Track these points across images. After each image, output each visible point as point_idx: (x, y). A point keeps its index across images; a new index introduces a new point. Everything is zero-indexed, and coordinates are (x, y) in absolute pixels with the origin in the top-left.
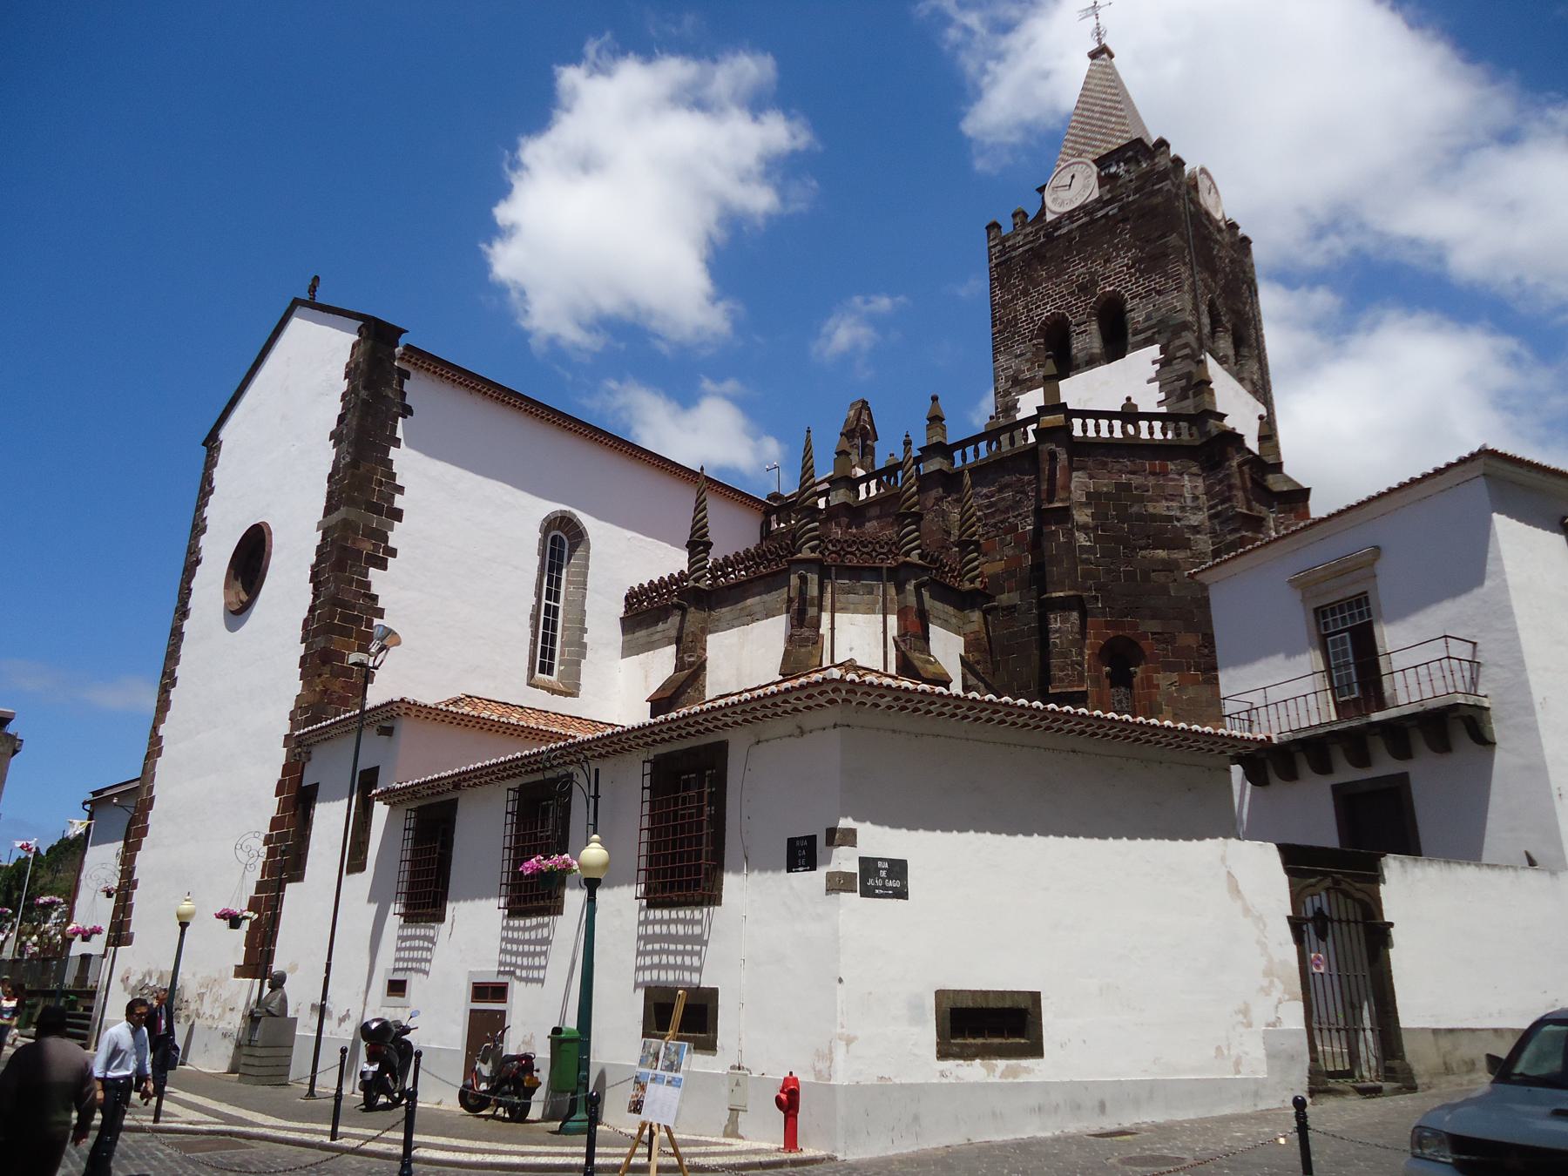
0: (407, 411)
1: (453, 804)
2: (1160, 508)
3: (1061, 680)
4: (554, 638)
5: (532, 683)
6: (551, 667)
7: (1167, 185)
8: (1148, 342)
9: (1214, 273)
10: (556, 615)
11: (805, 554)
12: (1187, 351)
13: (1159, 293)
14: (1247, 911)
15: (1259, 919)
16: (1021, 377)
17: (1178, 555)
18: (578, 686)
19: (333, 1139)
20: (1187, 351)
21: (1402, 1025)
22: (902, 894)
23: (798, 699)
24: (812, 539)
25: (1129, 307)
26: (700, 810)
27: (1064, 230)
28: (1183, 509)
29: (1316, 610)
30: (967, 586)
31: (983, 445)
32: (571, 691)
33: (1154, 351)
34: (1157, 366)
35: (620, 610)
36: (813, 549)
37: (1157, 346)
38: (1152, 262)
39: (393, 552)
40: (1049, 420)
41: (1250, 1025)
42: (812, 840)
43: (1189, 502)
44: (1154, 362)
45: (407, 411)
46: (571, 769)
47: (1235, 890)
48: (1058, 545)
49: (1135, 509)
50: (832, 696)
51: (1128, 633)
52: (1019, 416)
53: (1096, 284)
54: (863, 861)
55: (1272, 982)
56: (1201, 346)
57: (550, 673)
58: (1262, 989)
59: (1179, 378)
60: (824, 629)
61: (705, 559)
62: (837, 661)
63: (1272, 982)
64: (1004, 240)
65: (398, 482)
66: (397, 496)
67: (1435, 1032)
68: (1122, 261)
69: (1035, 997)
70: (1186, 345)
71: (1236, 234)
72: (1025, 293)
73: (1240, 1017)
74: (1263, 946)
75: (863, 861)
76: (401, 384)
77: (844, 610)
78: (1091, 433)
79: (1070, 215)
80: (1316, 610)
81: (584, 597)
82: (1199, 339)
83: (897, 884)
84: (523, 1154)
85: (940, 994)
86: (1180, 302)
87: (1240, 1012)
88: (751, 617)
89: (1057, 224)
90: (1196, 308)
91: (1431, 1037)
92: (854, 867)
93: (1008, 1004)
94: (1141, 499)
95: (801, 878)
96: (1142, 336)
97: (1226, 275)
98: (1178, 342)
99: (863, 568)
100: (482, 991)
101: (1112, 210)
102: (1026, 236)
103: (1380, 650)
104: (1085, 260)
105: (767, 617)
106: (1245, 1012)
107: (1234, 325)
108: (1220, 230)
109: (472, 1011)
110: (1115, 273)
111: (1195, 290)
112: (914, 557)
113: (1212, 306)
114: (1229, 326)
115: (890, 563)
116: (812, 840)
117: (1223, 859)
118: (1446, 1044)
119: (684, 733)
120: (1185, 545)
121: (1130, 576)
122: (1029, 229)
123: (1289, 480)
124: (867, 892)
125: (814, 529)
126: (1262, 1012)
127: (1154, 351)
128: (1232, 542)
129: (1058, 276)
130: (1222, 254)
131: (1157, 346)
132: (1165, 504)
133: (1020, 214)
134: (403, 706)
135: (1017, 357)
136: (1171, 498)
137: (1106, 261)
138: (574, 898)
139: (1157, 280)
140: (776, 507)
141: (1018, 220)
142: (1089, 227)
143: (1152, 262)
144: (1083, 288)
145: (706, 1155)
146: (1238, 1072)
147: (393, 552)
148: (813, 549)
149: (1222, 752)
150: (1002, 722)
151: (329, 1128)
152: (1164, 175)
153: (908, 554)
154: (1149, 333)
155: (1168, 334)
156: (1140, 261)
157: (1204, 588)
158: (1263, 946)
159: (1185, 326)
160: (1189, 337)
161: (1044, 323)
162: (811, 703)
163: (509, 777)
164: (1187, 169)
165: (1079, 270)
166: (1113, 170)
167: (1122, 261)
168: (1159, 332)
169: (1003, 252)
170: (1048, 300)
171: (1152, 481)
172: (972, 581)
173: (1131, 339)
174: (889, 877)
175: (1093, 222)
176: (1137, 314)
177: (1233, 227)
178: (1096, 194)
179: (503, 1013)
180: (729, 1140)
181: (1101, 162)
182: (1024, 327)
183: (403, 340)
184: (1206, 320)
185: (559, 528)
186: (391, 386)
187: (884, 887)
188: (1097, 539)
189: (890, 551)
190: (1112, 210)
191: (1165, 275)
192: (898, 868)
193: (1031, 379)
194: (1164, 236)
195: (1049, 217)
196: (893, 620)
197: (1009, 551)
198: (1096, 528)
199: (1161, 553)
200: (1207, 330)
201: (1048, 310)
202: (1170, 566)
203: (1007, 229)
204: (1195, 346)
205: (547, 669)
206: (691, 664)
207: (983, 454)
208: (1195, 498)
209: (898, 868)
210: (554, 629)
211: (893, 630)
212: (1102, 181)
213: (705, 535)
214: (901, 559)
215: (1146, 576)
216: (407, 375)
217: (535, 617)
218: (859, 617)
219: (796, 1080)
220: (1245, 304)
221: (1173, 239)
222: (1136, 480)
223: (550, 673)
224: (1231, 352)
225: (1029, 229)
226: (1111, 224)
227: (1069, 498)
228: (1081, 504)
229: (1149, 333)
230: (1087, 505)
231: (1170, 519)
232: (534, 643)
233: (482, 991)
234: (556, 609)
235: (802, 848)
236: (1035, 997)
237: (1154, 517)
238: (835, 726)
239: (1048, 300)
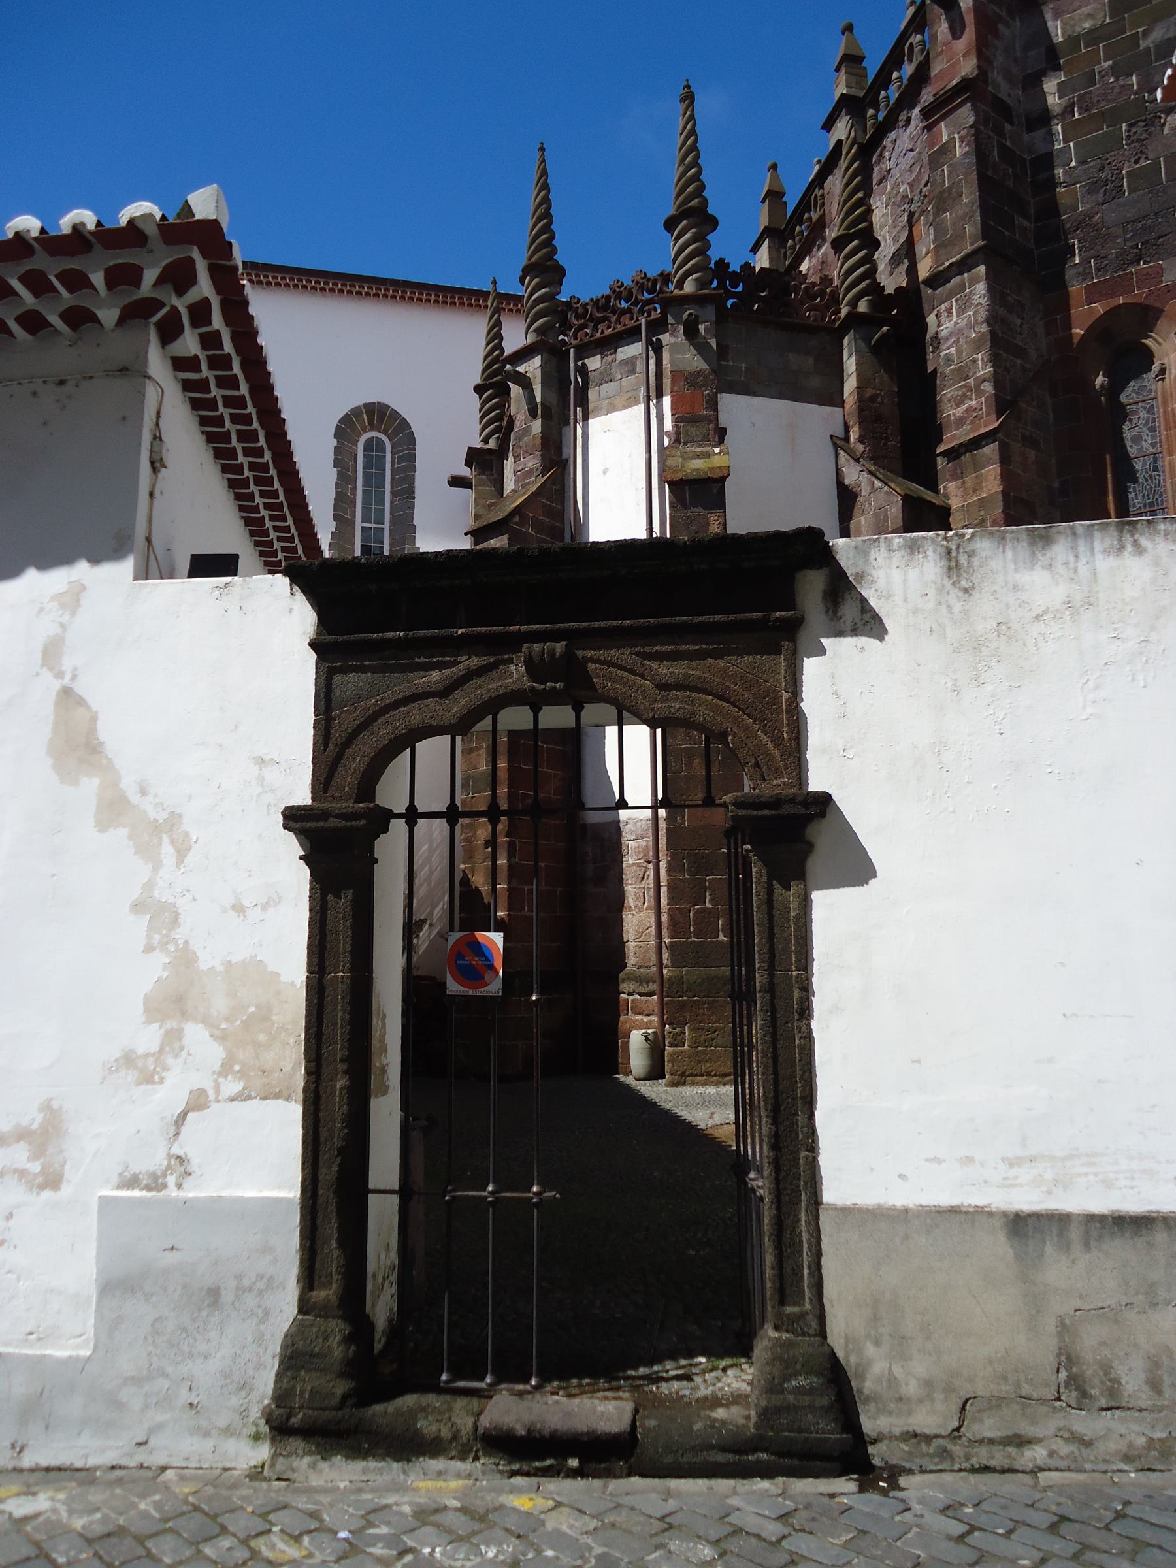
3: (960, 422)
15: (161, 834)
21: (832, 1192)
41: (52, 1181)
51: (1139, 294)
55: (173, 1039)
58: (128, 1059)
63: (173, 1039)
67: (1020, 1225)
73: (19, 1155)
74: (161, 916)
87: (22, 1135)
91: (1000, 1246)
99: (621, 333)
106: (45, 1135)
117: (51, 653)
118: (1067, 1274)
126: (112, 1136)
153: (680, 285)
158: (161, 916)
172: (854, 303)
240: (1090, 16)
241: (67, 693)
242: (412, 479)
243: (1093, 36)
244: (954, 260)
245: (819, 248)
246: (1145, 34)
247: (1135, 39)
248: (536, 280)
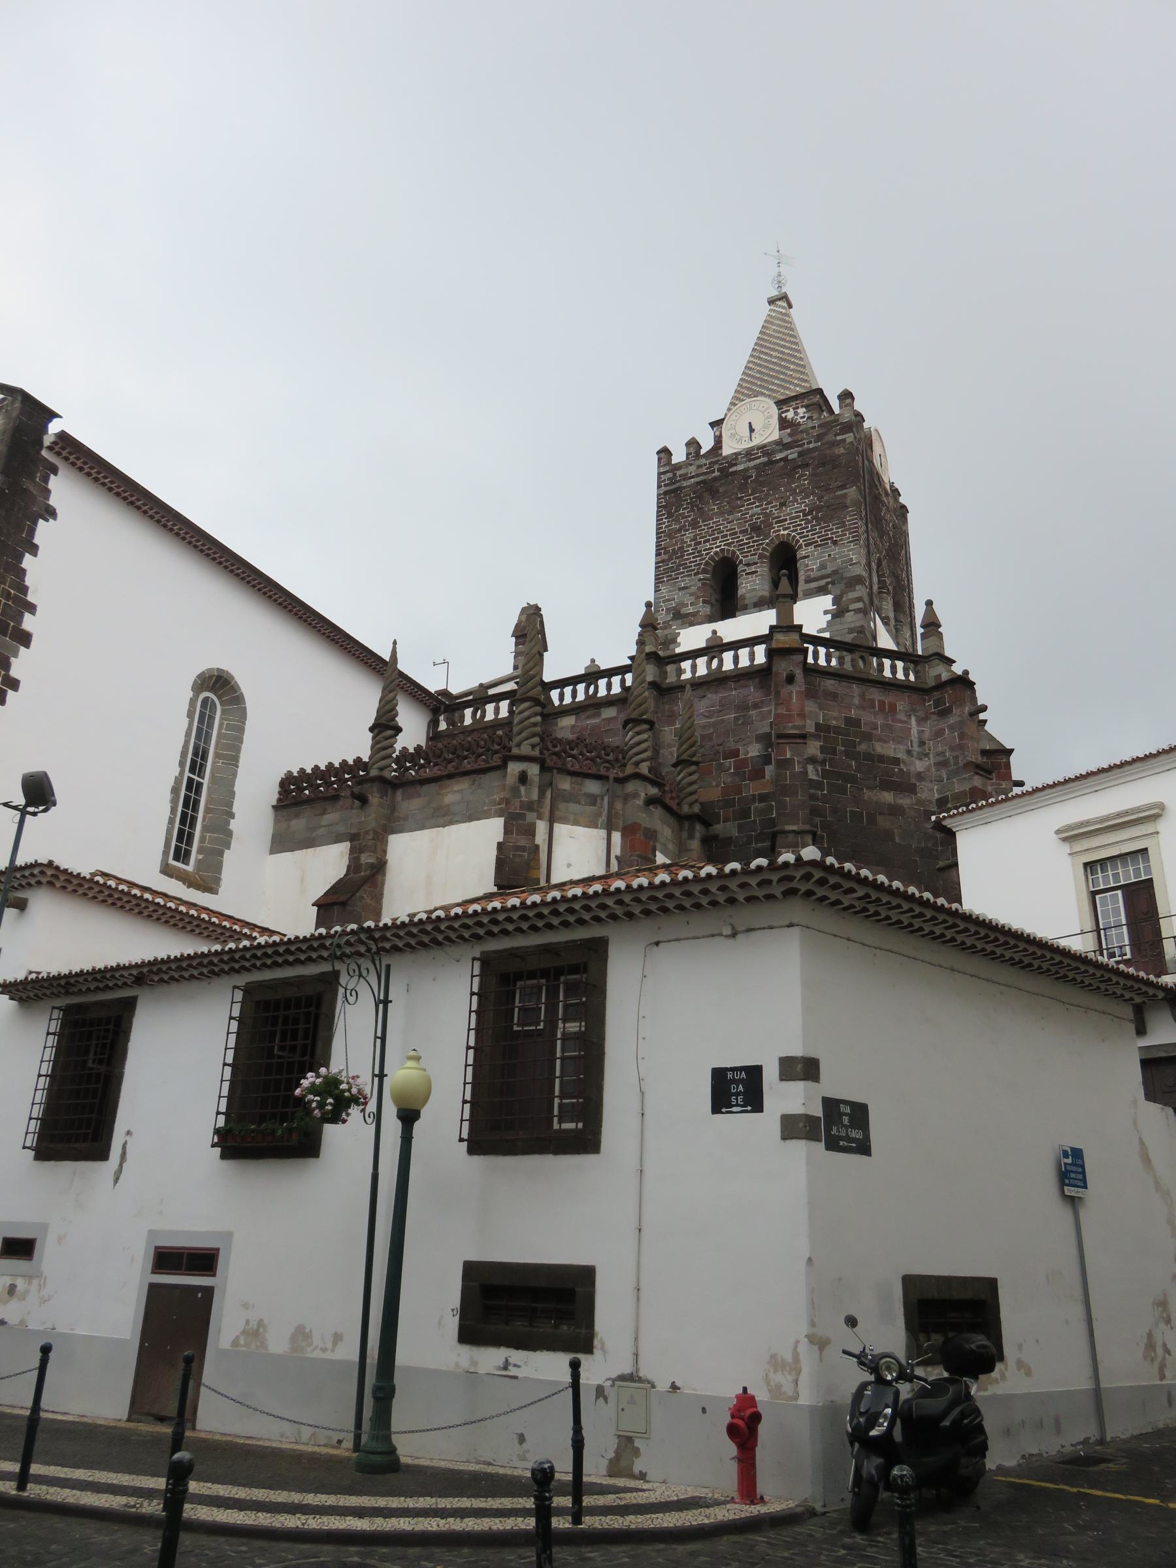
0: (51, 513)
1: (128, 1006)
2: (888, 749)
4: (194, 820)
5: (166, 871)
6: (187, 854)
7: (849, 437)
8: (822, 591)
9: (882, 533)
10: (198, 792)
11: (525, 750)
12: (860, 605)
13: (835, 543)
14: (1157, 1184)
16: (684, 611)
17: (905, 801)
18: (218, 881)
19: (21, 1487)
20: (860, 605)
22: (863, 1148)
23: (743, 886)
24: (534, 735)
25: (802, 553)
26: (552, 1024)
27: (740, 467)
28: (909, 752)
29: (1086, 865)
30: (685, 809)
31: (581, 688)
32: (209, 885)
33: (826, 602)
34: (829, 617)
35: (273, 796)
36: (533, 746)
37: (829, 598)
38: (826, 512)
39: (14, 684)
40: (782, 640)
42: (755, 1073)
43: (915, 744)
44: (826, 612)
45: (51, 513)
46: (338, 966)
47: (1146, 1160)
48: (793, 775)
49: (862, 747)
50: (794, 884)
52: (678, 650)
53: (770, 526)
54: (830, 1104)
56: (872, 603)
57: (186, 861)
59: (851, 631)
60: (541, 838)
61: (391, 746)
62: (555, 880)
64: (678, 466)
65: (31, 598)
66: (27, 616)
68: (798, 506)
69: (991, 1284)
70: (859, 599)
71: (896, 500)
72: (694, 525)
75: (830, 1104)
76: (46, 480)
77: (564, 821)
78: (822, 662)
79: (749, 454)
80: (1086, 865)
81: (235, 775)
82: (871, 595)
83: (856, 1134)
84: (359, 1513)
85: (909, 1282)
86: (851, 555)
88: (443, 817)
89: (734, 458)
90: (869, 564)
92: (818, 1111)
93: (967, 1295)
94: (868, 737)
95: (738, 1122)
96: (814, 585)
97: (890, 540)
98: (852, 595)
100: (166, 1259)
101: (792, 454)
102: (699, 467)
103: (1162, 912)
104: (760, 499)
105: (470, 818)
107: (894, 589)
108: (887, 494)
109: (153, 1289)
110: (790, 519)
111: (868, 547)
112: (644, 769)
113: (879, 564)
114: (890, 588)
115: (614, 773)
116: (755, 1073)
117: (1135, 1122)
119: (303, 957)
120: (912, 789)
121: (857, 817)
122: (703, 461)
123: (992, 739)
124: (833, 1145)
125: (535, 725)
127: (826, 602)
128: (963, 793)
129: (730, 513)
130: (888, 517)
131: (829, 598)
132: (892, 745)
133: (693, 444)
134: (49, 872)
135: (680, 589)
136: (899, 740)
137: (783, 504)
138: (347, 1140)
139: (834, 530)
140: (440, 705)
141: (692, 450)
142: (764, 472)
143: (826, 512)
144: (756, 529)
145: (624, 1510)
146: (1163, 1377)
147: (14, 684)
148: (533, 746)
149: (1132, 999)
150: (953, 939)
151: (15, 1467)
152: (848, 427)
153: (637, 764)
154: (822, 583)
155: (842, 586)
156: (818, 509)
157: (951, 835)
159: (859, 580)
160: (861, 591)
161: (712, 558)
162: (760, 893)
163: (232, 970)
164: (866, 425)
165: (754, 510)
166: (790, 415)
167: (798, 506)
168: (833, 583)
169: (672, 481)
170: (721, 534)
171: (880, 722)
172: (691, 805)
173: (802, 586)
174: (853, 1125)
175: (771, 463)
176: (811, 561)
177: (896, 492)
178: (775, 435)
179: (209, 1292)
180: (621, 1482)
181: (780, 403)
182: (689, 558)
183: (54, 427)
184: (875, 579)
185: (212, 689)
186: (34, 481)
187: (848, 1139)
188: (825, 774)
189: (617, 760)
190: (792, 454)
191: (843, 525)
192: (860, 1113)
193: (694, 614)
194: (842, 487)
195: (727, 451)
196: (617, 837)
197: (726, 779)
198: (823, 762)
199: (888, 797)
200: (875, 587)
201: (716, 548)
202: (895, 811)
203: (679, 456)
204: (867, 602)
205: (182, 855)
206: (372, 866)
207: (581, 697)
208: (922, 743)
209: (860, 1113)
210: (195, 809)
211: (616, 850)
212: (784, 423)
213: (393, 719)
214: (629, 770)
215: (872, 820)
216: (55, 471)
217: (175, 790)
218: (580, 831)
219: (752, 1398)
220: (902, 570)
221: (852, 492)
222: (866, 717)
223: (186, 861)
224: (891, 615)
225: (703, 461)
226: (791, 469)
227: (804, 726)
228: (811, 735)
229: (822, 583)
230: (816, 737)
231: (897, 761)
232: (171, 821)
233: (166, 1259)
234: (200, 785)
235: (737, 1082)
236: (991, 1284)
237: (881, 758)
238: (791, 925)
239: (721, 534)
240: (835, 718)
241: (1140, 1139)
242: (238, 750)
243: (837, 730)
244: (794, 828)
245: (588, 718)
246: (860, 743)
247: (854, 744)
248: (532, 710)
